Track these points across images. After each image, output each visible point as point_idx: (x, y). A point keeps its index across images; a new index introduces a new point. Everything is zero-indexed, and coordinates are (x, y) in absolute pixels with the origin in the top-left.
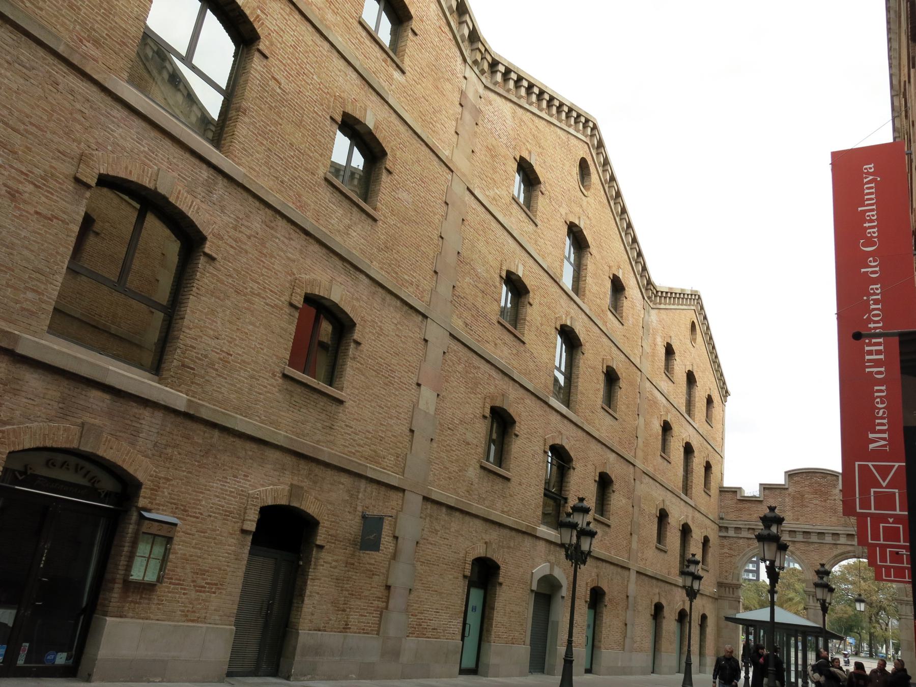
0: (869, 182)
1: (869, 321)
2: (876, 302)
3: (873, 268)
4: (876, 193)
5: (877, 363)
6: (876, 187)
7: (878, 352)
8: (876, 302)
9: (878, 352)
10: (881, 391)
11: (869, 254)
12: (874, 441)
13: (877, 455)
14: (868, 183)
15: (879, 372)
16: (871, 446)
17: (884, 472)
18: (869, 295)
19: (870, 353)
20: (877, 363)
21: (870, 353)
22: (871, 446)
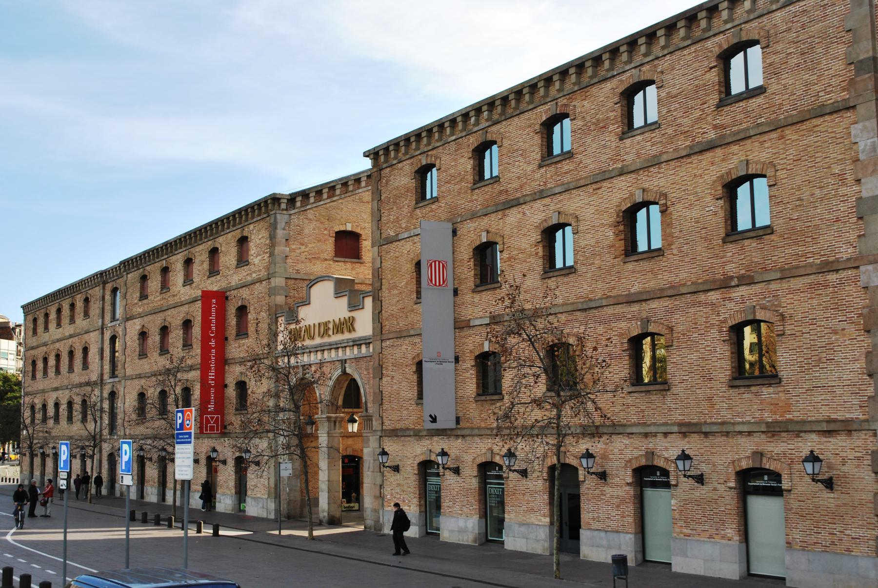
0: (213, 307)
1: (211, 363)
2: (213, 356)
3: (213, 343)
4: (216, 312)
5: (212, 380)
6: (216, 310)
7: (213, 376)
8: (213, 356)
9: (213, 376)
10: (212, 390)
11: (213, 337)
12: (210, 408)
13: (210, 413)
14: (213, 307)
15: (212, 383)
16: (209, 410)
17: (213, 418)
18: (211, 353)
19: (210, 376)
20: (212, 380)
21: (210, 376)
22: (209, 410)
